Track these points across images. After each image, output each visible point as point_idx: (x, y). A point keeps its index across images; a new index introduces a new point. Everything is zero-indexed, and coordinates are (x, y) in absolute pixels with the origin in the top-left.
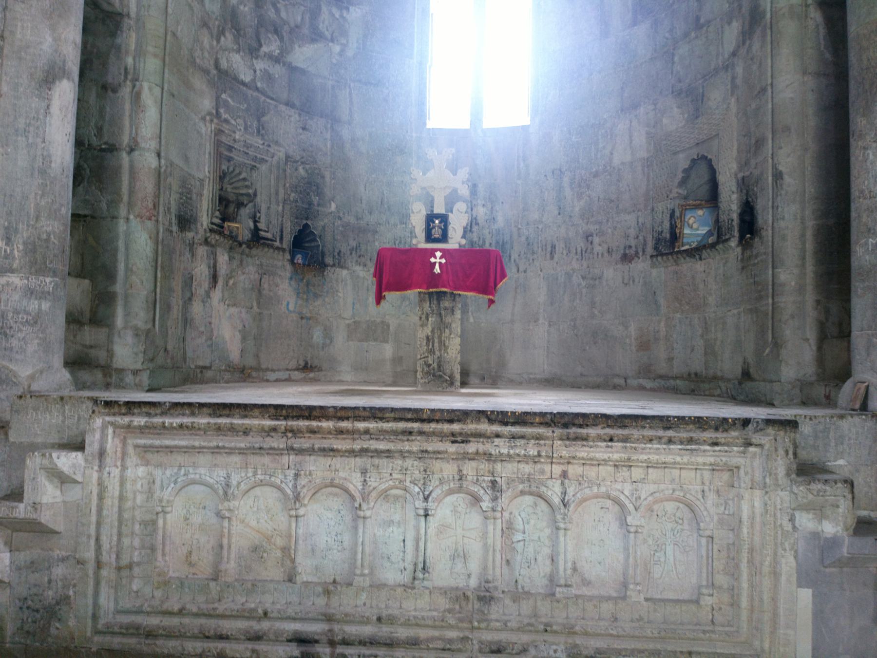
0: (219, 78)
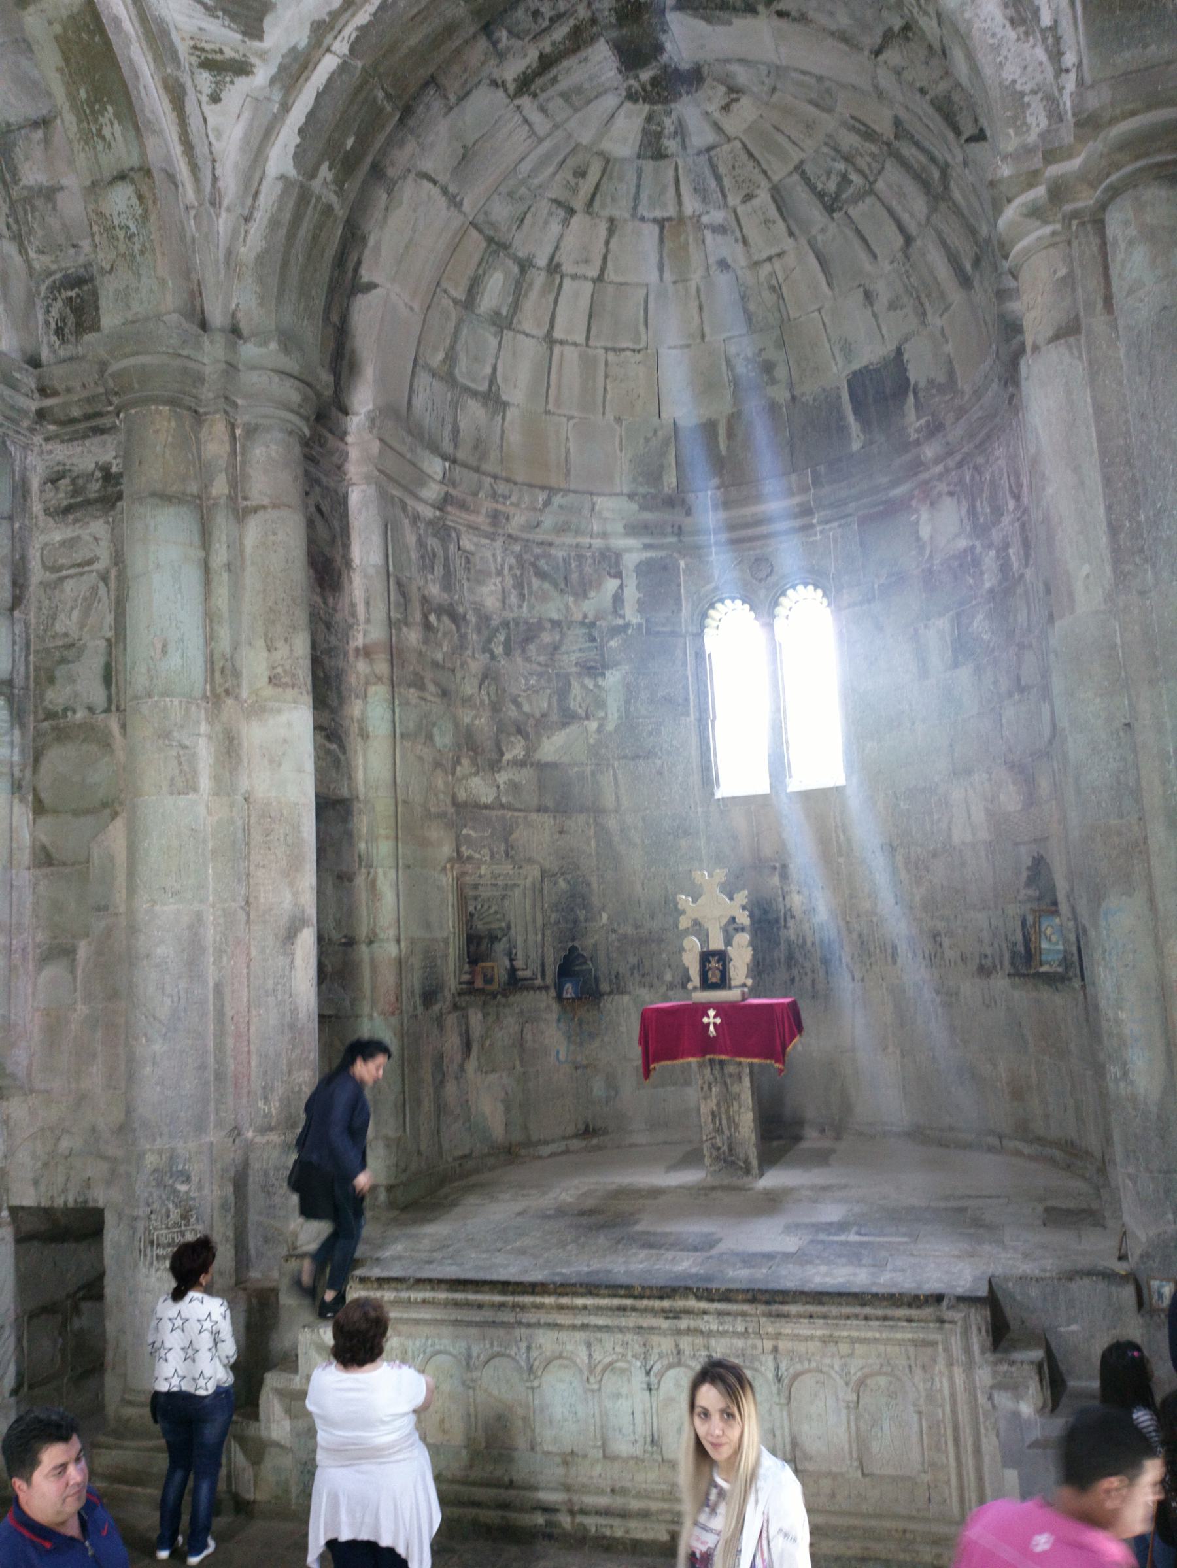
0: (458, 813)
